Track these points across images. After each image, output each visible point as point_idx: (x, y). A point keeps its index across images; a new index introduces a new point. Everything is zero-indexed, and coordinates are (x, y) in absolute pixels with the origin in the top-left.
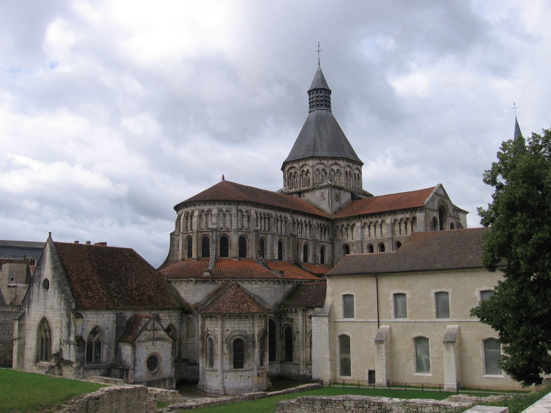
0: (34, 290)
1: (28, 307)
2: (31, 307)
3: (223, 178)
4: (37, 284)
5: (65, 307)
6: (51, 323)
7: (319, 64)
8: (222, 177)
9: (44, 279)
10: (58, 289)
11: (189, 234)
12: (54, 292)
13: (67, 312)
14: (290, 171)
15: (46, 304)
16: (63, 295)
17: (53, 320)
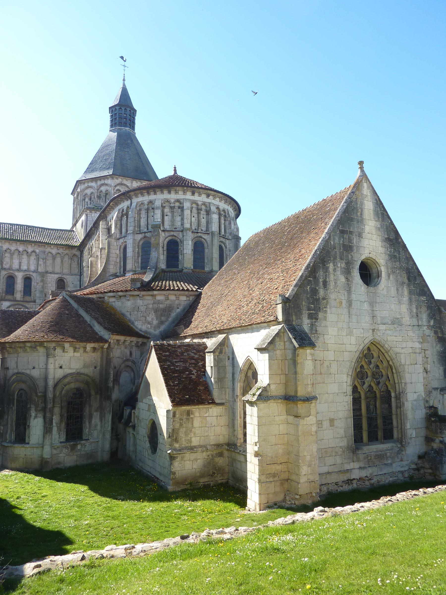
0: (332, 277)
1: (313, 317)
2: (325, 318)
3: (175, 170)
4: (341, 265)
5: (432, 323)
6: (396, 354)
7: (124, 80)
8: (174, 169)
9: (363, 257)
10: (409, 285)
11: (199, 234)
12: (397, 290)
13: (436, 333)
14: (118, 188)
15: (378, 313)
16: (423, 298)
17: (402, 348)
